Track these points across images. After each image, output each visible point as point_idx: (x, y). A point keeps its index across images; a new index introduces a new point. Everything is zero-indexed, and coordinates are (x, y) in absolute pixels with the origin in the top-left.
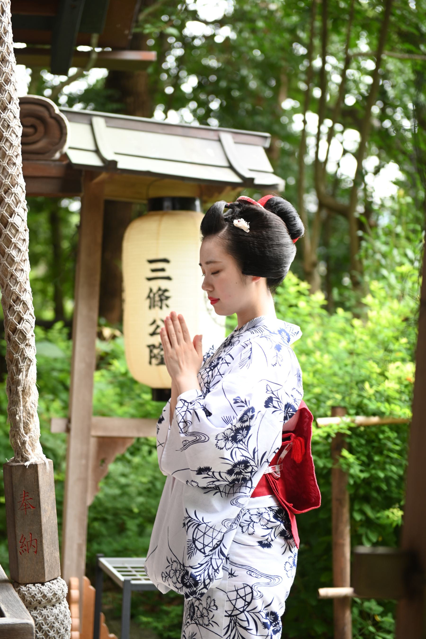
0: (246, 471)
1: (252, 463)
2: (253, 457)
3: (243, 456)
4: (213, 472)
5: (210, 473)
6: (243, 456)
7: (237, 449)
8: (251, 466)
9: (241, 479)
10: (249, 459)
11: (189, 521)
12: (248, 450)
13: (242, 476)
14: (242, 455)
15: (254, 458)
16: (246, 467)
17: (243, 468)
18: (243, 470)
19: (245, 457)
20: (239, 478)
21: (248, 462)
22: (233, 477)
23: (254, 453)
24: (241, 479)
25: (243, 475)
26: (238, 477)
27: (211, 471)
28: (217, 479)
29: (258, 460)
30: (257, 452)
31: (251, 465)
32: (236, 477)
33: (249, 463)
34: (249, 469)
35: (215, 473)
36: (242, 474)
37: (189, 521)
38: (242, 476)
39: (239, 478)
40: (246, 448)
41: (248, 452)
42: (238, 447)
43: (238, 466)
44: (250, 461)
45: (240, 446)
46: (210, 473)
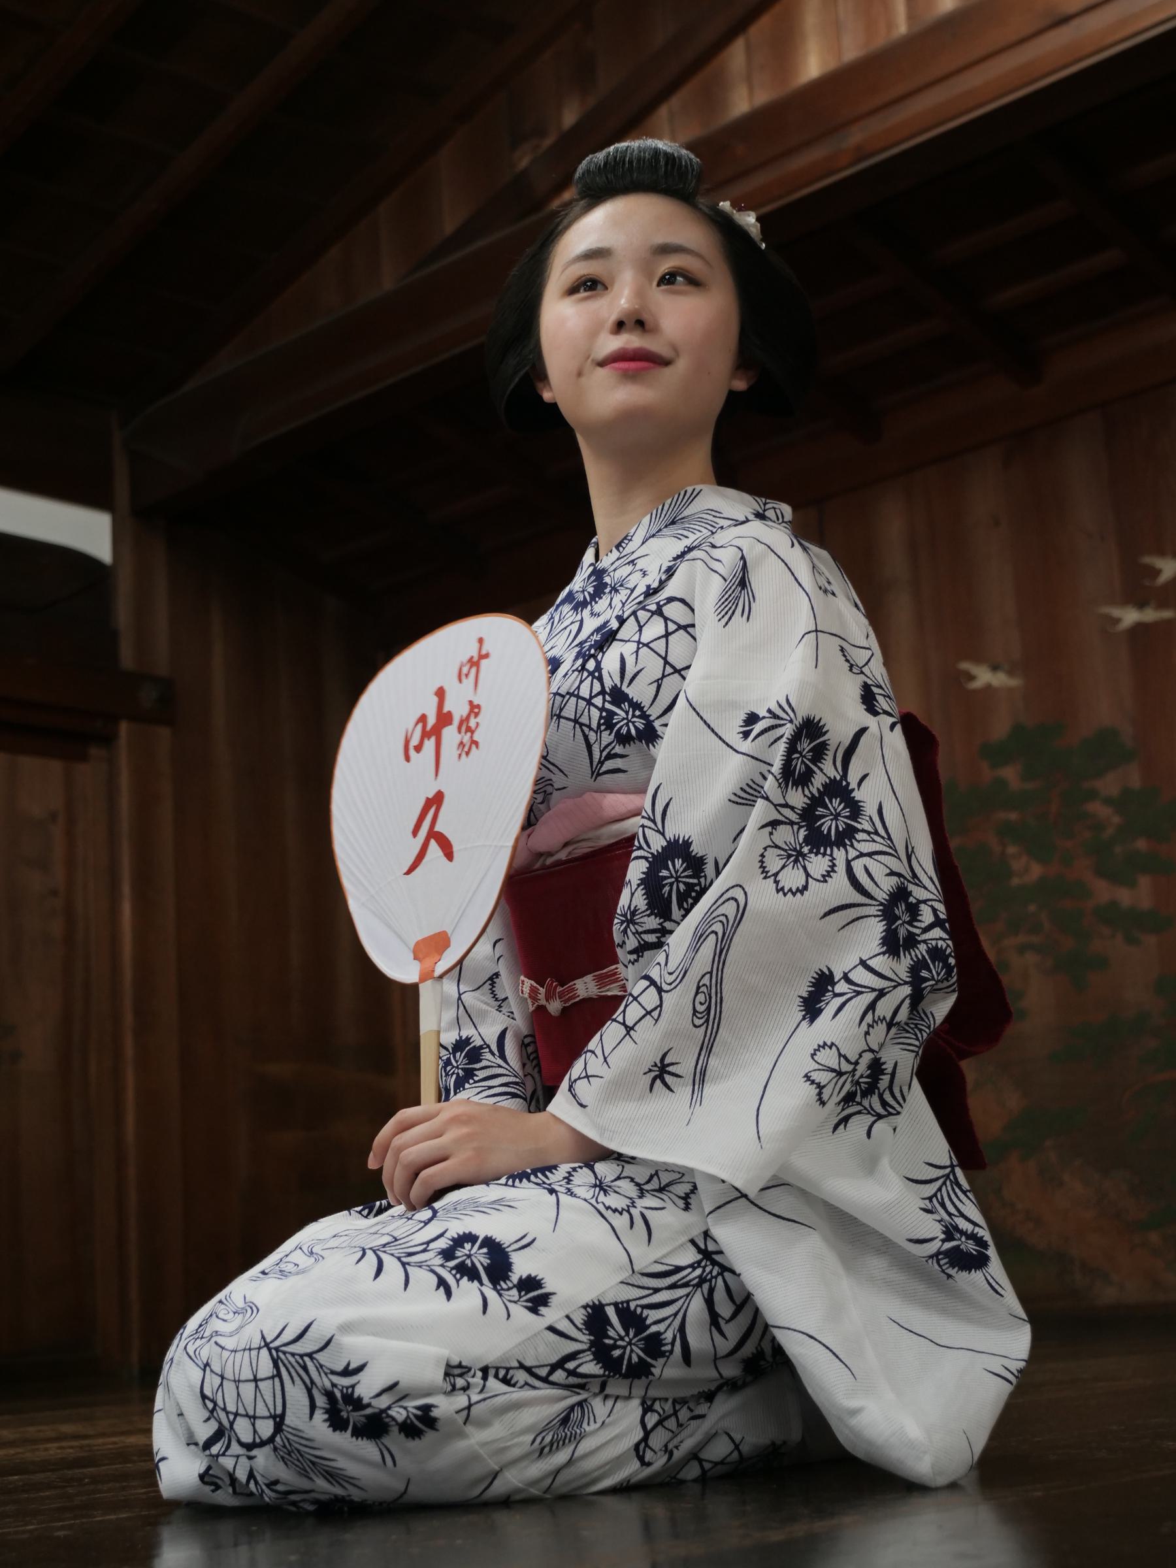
0: (923, 925)
7: (866, 860)
9: (927, 957)
14: (888, 871)
20: (920, 957)
22: (906, 961)
24: (927, 957)
25: (925, 941)
26: (916, 956)
32: (912, 959)
36: (919, 942)
38: (923, 948)
39: (920, 957)
40: (891, 847)
42: (862, 855)
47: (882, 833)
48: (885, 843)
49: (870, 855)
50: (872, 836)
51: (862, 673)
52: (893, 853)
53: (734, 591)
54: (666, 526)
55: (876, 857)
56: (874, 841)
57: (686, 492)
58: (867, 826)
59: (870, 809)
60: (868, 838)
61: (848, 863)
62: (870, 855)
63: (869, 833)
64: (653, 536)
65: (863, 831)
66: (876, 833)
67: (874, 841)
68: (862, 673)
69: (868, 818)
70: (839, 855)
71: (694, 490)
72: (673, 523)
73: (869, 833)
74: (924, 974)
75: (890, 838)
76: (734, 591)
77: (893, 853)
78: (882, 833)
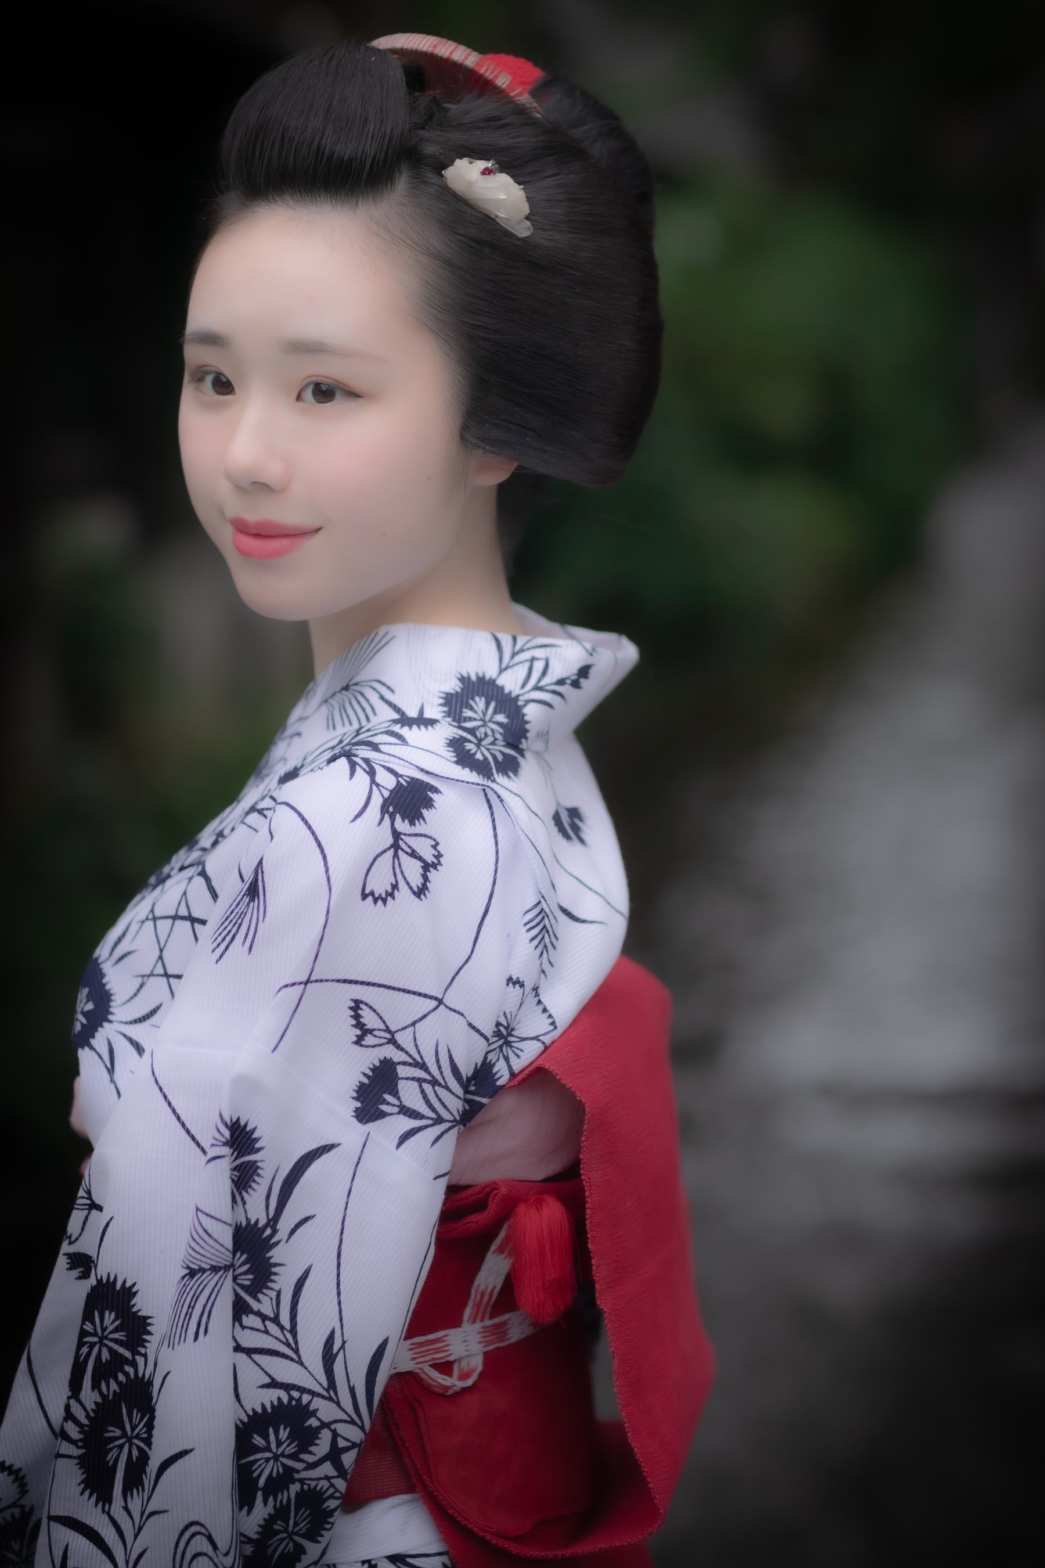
1: (325, 1410)
3: (274, 1384)
6: (274, 1384)
12: (296, 1351)
14: (267, 1380)
15: (332, 1385)
16: (305, 1438)
19: (287, 1387)
21: (307, 1412)
23: (329, 1358)
25: (302, 1481)
34: (322, 1446)
36: (293, 1481)
38: (294, 1488)
41: (302, 1364)
44: (317, 1403)
47: (285, 1319)
48: (282, 1337)
49: (249, 1352)
50: (267, 1323)
51: (392, 1041)
52: (290, 1353)
53: (238, 904)
54: (340, 692)
55: (256, 1357)
56: (266, 1332)
57: (376, 634)
58: (267, 1308)
59: (284, 1281)
60: (261, 1326)
62: (249, 1352)
63: (264, 1318)
64: (326, 701)
65: (258, 1314)
66: (276, 1320)
68: (392, 1041)
69: (273, 1294)
71: (387, 633)
72: (346, 688)
73: (264, 1318)
76: (238, 904)
77: (290, 1353)
78: (285, 1319)
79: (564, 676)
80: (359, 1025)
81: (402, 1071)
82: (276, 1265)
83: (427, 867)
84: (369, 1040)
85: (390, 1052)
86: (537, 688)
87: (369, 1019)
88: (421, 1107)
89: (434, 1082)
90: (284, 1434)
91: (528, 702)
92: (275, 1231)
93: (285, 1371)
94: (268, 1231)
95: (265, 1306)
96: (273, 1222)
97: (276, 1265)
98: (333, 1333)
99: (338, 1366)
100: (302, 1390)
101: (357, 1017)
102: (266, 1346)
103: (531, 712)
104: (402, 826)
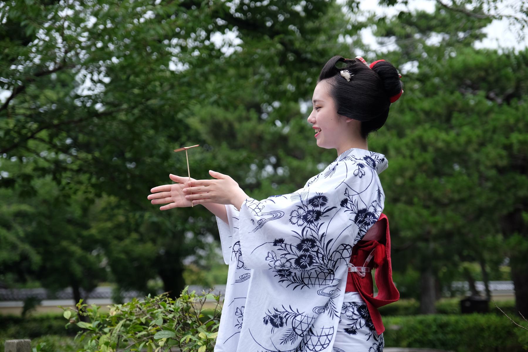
0: (313, 250)
1: (318, 243)
2: (320, 240)
3: (312, 236)
4: (286, 244)
5: (283, 245)
6: (312, 236)
7: (309, 229)
8: (318, 246)
9: (307, 256)
10: (316, 240)
11: (287, 314)
12: (318, 233)
13: (309, 253)
14: (312, 235)
15: (321, 240)
16: (313, 246)
17: (310, 246)
18: (310, 248)
19: (314, 237)
20: (306, 254)
22: (301, 253)
24: (307, 256)
25: (310, 253)
26: (305, 254)
27: (284, 243)
28: (288, 252)
29: (324, 244)
30: (324, 237)
31: (317, 246)
32: (304, 254)
33: (316, 243)
34: (316, 249)
35: (287, 245)
36: (309, 252)
37: (287, 314)
38: (309, 253)
39: (306, 254)
40: (317, 231)
42: (310, 228)
43: (306, 242)
44: (317, 242)
45: (311, 227)
46: (283, 245)
47: (318, 227)
49: (311, 229)
51: (349, 196)
52: (317, 232)
55: (312, 230)
56: (315, 227)
58: (316, 224)
61: (305, 227)
62: (311, 229)
63: (315, 225)
65: (314, 224)
66: (317, 227)
67: (315, 227)
68: (349, 196)
69: (318, 223)
70: (306, 224)
73: (315, 225)
74: (304, 258)
75: (319, 230)
77: (317, 232)
78: (318, 227)
79: (381, 159)
80: (346, 192)
81: (348, 201)
82: (319, 219)
83: (362, 174)
84: (346, 195)
85: (348, 198)
86: (377, 159)
87: (347, 192)
88: (350, 208)
89: (353, 205)
90: (310, 243)
91: (376, 161)
92: (323, 214)
93: (315, 235)
94: (322, 214)
95: (316, 223)
96: (323, 213)
97: (319, 219)
98: (324, 233)
99: (323, 238)
100: (316, 239)
101: (346, 190)
102: (314, 229)
103: (376, 162)
104: (360, 168)
